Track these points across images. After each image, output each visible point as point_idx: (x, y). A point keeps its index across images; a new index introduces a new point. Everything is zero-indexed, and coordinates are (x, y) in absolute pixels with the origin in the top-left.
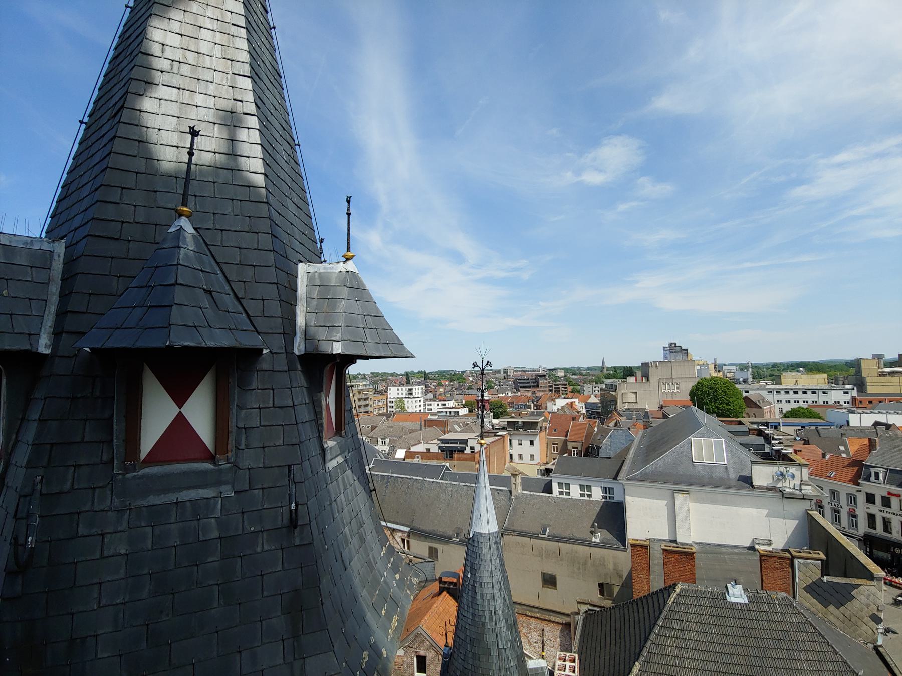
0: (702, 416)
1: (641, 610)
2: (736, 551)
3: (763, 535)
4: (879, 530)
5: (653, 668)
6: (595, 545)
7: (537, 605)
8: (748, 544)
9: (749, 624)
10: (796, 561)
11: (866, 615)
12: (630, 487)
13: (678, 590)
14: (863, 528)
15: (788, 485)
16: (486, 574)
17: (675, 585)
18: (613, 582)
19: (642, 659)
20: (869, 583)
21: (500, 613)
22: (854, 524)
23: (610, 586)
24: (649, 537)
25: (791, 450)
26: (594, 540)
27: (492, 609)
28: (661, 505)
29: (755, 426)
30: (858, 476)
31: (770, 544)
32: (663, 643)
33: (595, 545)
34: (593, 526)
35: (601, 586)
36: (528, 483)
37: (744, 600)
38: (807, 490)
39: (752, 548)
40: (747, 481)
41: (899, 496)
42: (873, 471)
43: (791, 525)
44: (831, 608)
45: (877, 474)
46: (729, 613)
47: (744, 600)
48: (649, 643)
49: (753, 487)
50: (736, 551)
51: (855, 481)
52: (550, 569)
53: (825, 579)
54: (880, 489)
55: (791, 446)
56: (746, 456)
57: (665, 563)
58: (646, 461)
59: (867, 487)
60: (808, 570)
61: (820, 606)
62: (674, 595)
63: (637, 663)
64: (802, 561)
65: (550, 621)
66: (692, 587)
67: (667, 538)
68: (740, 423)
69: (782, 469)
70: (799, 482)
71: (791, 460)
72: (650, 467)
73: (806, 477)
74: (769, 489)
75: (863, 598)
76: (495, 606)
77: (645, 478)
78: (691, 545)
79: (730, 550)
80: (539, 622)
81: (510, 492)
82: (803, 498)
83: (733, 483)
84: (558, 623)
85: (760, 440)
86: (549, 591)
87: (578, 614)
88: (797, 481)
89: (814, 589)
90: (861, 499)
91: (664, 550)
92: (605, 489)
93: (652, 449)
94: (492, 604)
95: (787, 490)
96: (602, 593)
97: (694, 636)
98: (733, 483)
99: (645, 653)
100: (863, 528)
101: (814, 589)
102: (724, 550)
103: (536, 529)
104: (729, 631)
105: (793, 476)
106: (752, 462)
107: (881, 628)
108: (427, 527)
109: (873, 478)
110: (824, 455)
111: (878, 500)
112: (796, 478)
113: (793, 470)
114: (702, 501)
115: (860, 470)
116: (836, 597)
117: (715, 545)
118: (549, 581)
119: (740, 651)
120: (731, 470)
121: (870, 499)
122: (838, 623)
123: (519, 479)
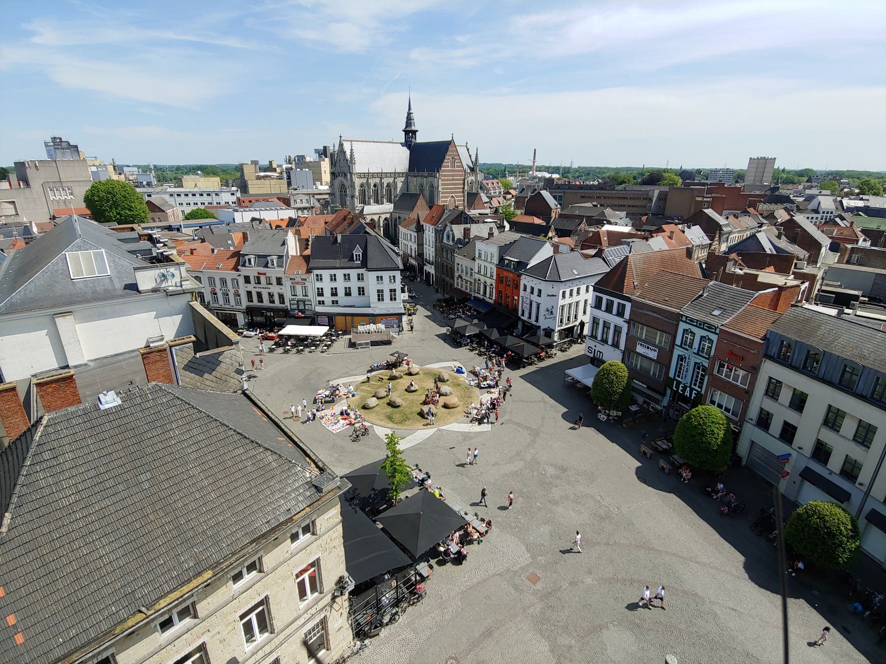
1: (10, 459)
2: (133, 354)
3: (155, 334)
4: (255, 302)
9: (126, 420)
10: (173, 349)
14: (245, 303)
15: (170, 285)
17: (41, 418)
19: (12, 506)
20: (230, 348)
22: (239, 303)
24: (34, 373)
25: (174, 252)
28: (41, 337)
29: (146, 232)
30: (237, 264)
31: (162, 339)
38: (188, 285)
39: (148, 346)
40: (133, 287)
42: (247, 258)
43: (178, 318)
44: (206, 375)
45: (250, 260)
49: (139, 292)
53: (198, 355)
54: (251, 271)
55: (175, 248)
56: (129, 262)
58: (14, 289)
59: (245, 271)
60: (184, 355)
61: (197, 377)
62: (41, 429)
64: (177, 348)
68: (132, 229)
69: (163, 271)
70: (179, 280)
74: (155, 291)
75: (227, 360)
78: (86, 365)
79: (127, 356)
82: (184, 292)
83: (121, 292)
88: (177, 279)
89: (193, 367)
90: (241, 280)
95: (170, 288)
98: (121, 292)
99: (15, 499)
100: (245, 303)
101: (193, 367)
102: (121, 358)
105: (173, 275)
106: (136, 269)
107: (244, 376)
109: (247, 264)
110: (213, 251)
112: (177, 277)
113: (172, 270)
114: (103, 316)
115: (239, 260)
117: (112, 356)
119: (118, 447)
120: (116, 281)
121: (247, 280)
122: (213, 385)
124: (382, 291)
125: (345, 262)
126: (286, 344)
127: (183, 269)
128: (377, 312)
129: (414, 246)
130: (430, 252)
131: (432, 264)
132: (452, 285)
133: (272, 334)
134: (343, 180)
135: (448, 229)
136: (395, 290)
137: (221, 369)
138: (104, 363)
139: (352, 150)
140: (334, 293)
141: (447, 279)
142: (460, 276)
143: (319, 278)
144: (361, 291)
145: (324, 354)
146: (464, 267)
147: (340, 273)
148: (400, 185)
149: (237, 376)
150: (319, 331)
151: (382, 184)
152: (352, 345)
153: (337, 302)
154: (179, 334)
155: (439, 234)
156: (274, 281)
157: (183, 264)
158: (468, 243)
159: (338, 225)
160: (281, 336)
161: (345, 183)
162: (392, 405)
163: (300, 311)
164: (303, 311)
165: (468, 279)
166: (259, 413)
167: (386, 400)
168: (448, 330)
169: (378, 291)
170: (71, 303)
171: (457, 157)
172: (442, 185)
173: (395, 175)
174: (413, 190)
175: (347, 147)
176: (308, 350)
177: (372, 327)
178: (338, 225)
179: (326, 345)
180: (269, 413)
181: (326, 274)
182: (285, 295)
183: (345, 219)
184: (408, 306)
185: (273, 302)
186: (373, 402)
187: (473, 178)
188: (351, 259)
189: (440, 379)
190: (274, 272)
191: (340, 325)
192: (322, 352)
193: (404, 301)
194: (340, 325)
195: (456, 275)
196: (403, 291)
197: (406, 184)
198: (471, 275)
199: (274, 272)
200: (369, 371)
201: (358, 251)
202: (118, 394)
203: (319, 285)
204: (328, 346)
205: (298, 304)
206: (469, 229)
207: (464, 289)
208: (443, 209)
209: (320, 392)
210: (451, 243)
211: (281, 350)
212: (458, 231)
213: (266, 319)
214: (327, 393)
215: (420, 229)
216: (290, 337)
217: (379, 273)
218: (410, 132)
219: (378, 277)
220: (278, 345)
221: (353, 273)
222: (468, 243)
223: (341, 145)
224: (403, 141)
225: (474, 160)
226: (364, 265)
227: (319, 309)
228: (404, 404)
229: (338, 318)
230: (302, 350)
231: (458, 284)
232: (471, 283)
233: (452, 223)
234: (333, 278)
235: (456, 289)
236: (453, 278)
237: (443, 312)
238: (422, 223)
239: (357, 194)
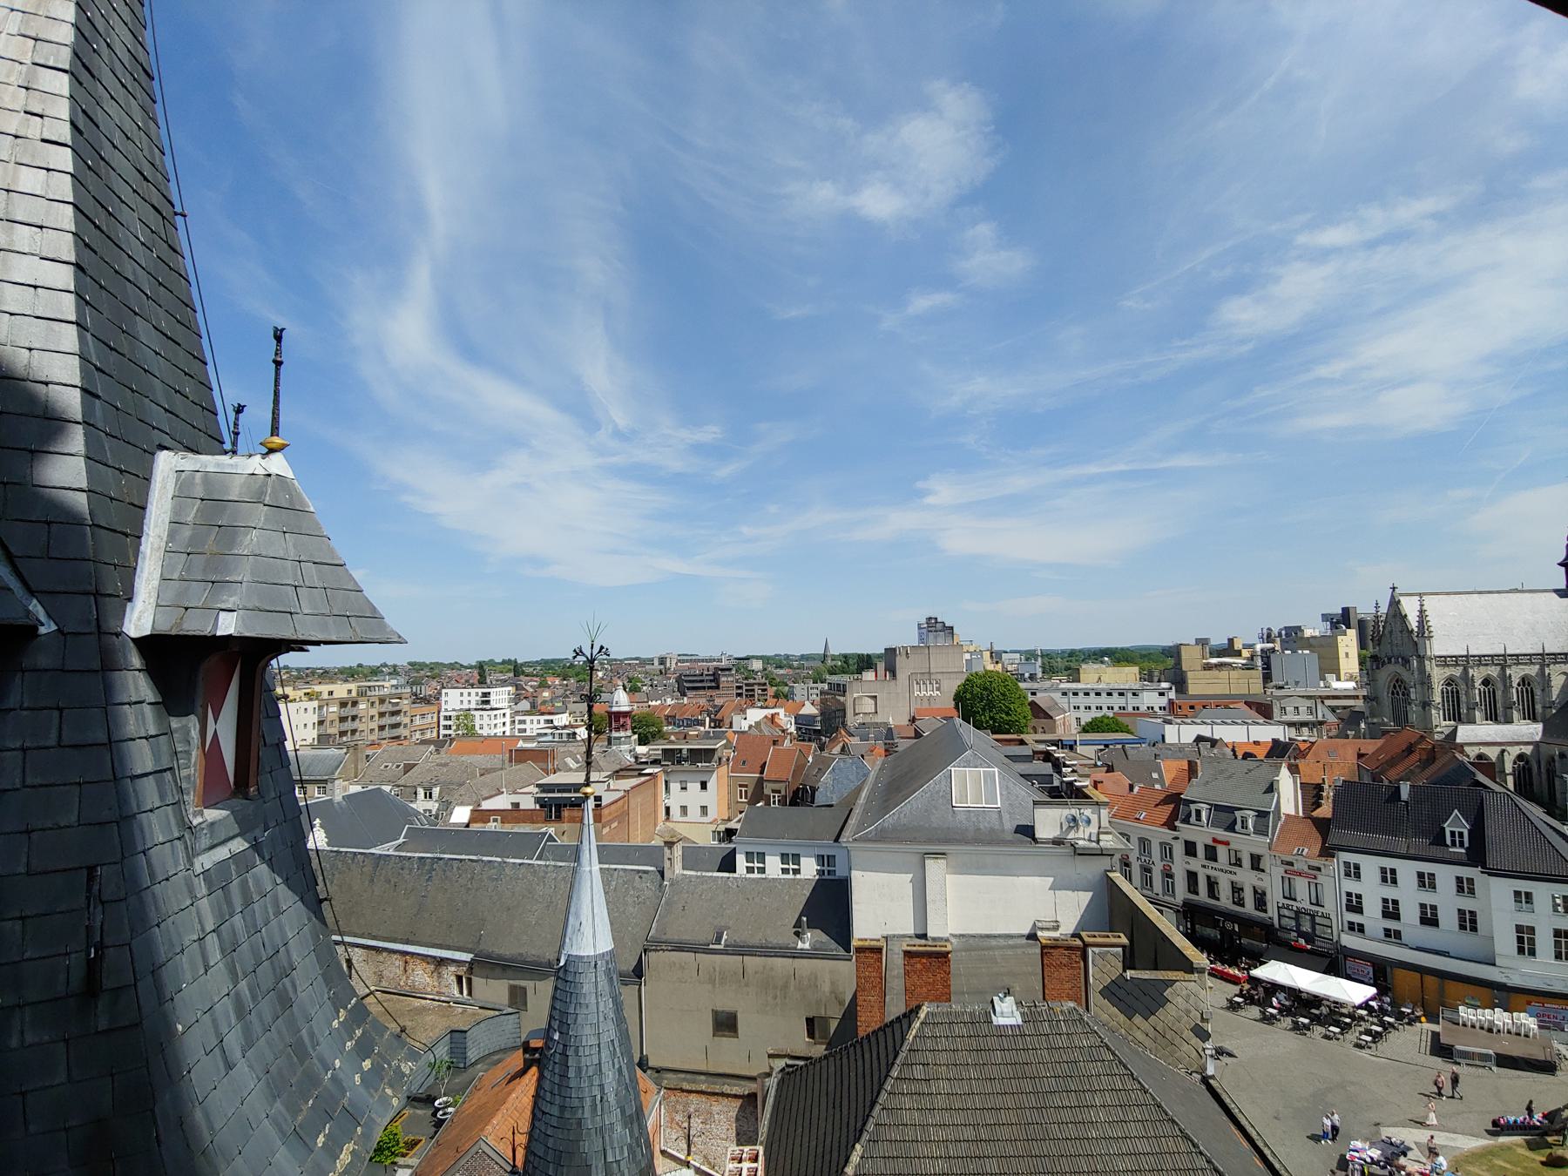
0: (968, 731)
1: (867, 1056)
2: (1011, 942)
3: (1046, 915)
4: (1203, 896)
5: (883, 1149)
6: (803, 955)
7: (703, 1068)
8: (1026, 931)
10: (1090, 950)
12: (859, 853)
13: (922, 1015)
14: (1181, 893)
16: (588, 1030)
17: (919, 1007)
18: (830, 1014)
19: (865, 1136)
20: (1187, 977)
21: (612, 1098)
22: (1169, 888)
23: (825, 1020)
26: (800, 945)
27: (596, 1092)
28: (902, 882)
29: (1042, 747)
31: (1056, 928)
32: (901, 1107)
33: (803, 955)
34: (798, 924)
35: (810, 1022)
36: (694, 857)
37: (1016, 1020)
38: (1108, 841)
39: (1032, 936)
40: (1027, 831)
41: (1227, 843)
42: (1193, 807)
43: (1085, 897)
44: (1138, 1019)
45: (1198, 813)
46: (993, 1042)
47: (1016, 1020)
48: (878, 1108)
49: (1035, 839)
50: (1011, 942)
51: (1170, 824)
52: (725, 1004)
53: (1129, 974)
54: (1202, 834)
55: (1088, 776)
56: (1026, 793)
57: (907, 973)
58: (885, 808)
59: (1187, 832)
60: (1105, 965)
61: (1122, 1018)
62: (916, 1025)
63: (858, 1146)
64: (1097, 950)
65: (723, 1095)
66: (944, 1007)
68: (1022, 742)
69: (1074, 811)
70: (1095, 831)
71: (1087, 797)
72: (889, 819)
73: (1105, 823)
74: (1057, 842)
75: (1180, 1000)
76: (601, 1086)
77: (882, 837)
79: (1002, 942)
80: (704, 1098)
81: (662, 873)
82: (1102, 853)
83: (1010, 836)
84: (735, 1096)
85: (1047, 768)
86: (726, 1042)
87: (769, 1075)
88: (1093, 829)
89: (1115, 992)
90: (1179, 849)
91: (907, 954)
92: (820, 859)
93: (896, 787)
94: (596, 1082)
95: (1081, 843)
96: (811, 1034)
97: (944, 1086)
99: (870, 1127)
100: (1181, 893)
101: (1115, 992)
102: (993, 942)
103: (703, 935)
104: (995, 1072)
105: (1089, 822)
108: (506, 948)
109: (1193, 819)
110: (1131, 788)
111: (1200, 851)
112: (1094, 826)
113: (1088, 812)
115: (1177, 808)
116: (1138, 1000)
117: (981, 936)
118: (726, 1024)
119: (1009, 1101)
120: (1006, 816)
121: (1190, 849)
122: (1148, 1042)
123: (678, 851)
125: (1421, 844)
126: (1264, 1003)
127: (1104, 812)
128: (1515, 980)
133: (1234, 971)
134: (1399, 669)
137: (1167, 1014)
138: (979, 943)
139: (1421, 611)
140: (1391, 910)
143: (1354, 872)
144: (1468, 921)
145: (1363, 1053)
147: (1407, 870)
149: (1195, 1041)
150: (1355, 993)
151: (1506, 680)
153: (1398, 934)
154: (1084, 924)
156: (1246, 862)
157: (1106, 804)
159: (1392, 762)
160: (1256, 982)
161: (1405, 675)
163: (1301, 934)
164: (1310, 938)
166: (1245, 1144)
170: (947, 841)
175: (1410, 608)
176: (1319, 1030)
177: (1500, 1017)
178: (1392, 762)
179: (1368, 1032)
180: (1267, 1151)
181: (1371, 866)
182: (1268, 897)
183: (1410, 750)
185: (1240, 902)
188: (1439, 839)
190: (1247, 843)
191: (1407, 991)
192: (1358, 1046)
194: (1407, 991)
199: (1247, 843)
201: (1456, 824)
202: (1019, 1004)
203: (1350, 886)
204: (1376, 1037)
205: (1297, 919)
209: (1358, 1144)
211: (1255, 1011)
213: (1234, 938)
214: (1375, 1153)
216: (1273, 988)
217: (1524, 886)
219: (1517, 894)
220: (1250, 1000)
221: (1446, 875)
223: (1395, 604)
226: (1477, 855)
227: (1350, 941)
230: (1306, 1027)
234: (1389, 877)
239: (1438, 699)
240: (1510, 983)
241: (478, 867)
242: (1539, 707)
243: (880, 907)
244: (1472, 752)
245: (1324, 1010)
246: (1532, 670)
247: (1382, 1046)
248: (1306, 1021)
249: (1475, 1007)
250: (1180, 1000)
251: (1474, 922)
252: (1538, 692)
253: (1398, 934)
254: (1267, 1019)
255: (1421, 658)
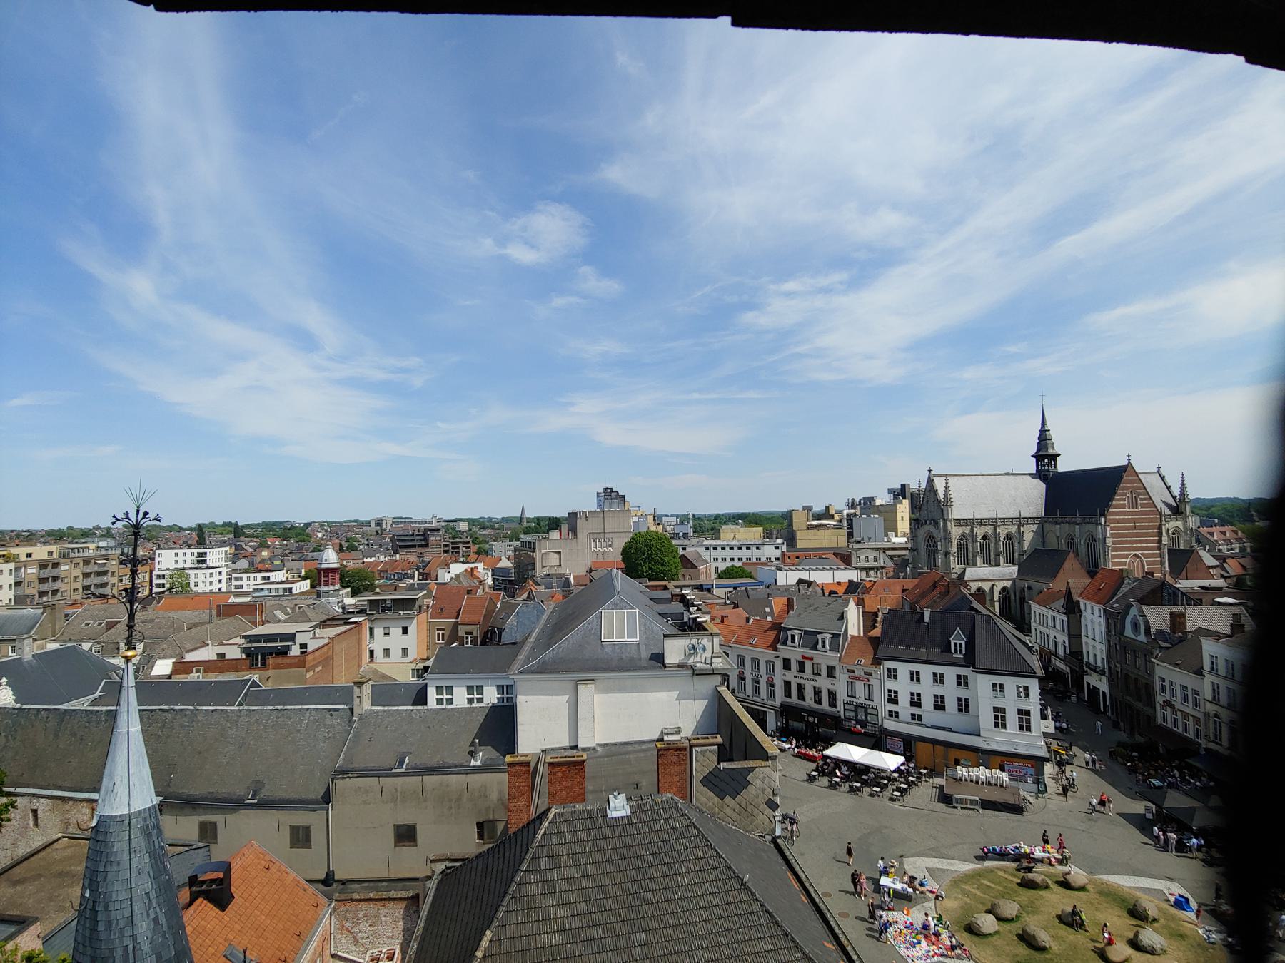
0: (621, 581)
2: (644, 747)
3: (671, 723)
4: (794, 699)
5: (511, 931)
6: (476, 770)
7: (385, 875)
8: (656, 737)
9: (630, 841)
11: (762, 799)
12: (522, 684)
13: (550, 816)
14: (780, 697)
15: (699, 660)
16: (118, 886)
18: (497, 817)
19: (496, 923)
20: (764, 763)
21: (146, 947)
22: (772, 695)
23: (493, 823)
24: (544, 747)
25: (708, 618)
26: (473, 763)
27: (128, 942)
28: (560, 702)
30: (776, 641)
32: (527, 892)
33: (476, 770)
34: (473, 744)
35: (480, 826)
36: (386, 693)
37: (626, 812)
38: (719, 663)
39: (661, 740)
40: (658, 658)
41: (811, 659)
42: (789, 633)
43: (701, 705)
44: (728, 799)
45: (793, 637)
46: (607, 832)
47: (626, 812)
48: (508, 897)
49: (664, 665)
50: (644, 747)
52: (405, 818)
53: (722, 765)
54: (794, 652)
57: (550, 781)
58: (549, 646)
59: (785, 652)
60: (705, 761)
61: (716, 799)
62: (546, 824)
63: (488, 932)
64: (699, 749)
65: (389, 899)
66: (579, 807)
67: (567, 744)
68: (665, 588)
69: (694, 641)
70: (709, 655)
71: (705, 630)
72: (549, 654)
73: (717, 649)
74: (681, 666)
75: (758, 781)
76: (134, 937)
77: (543, 669)
78: (594, 749)
79: (637, 747)
80: (372, 904)
81: (352, 710)
84: (401, 899)
85: (677, 607)
86: (407, 851)
87: (430, 878)
88: (708, 654)
90: (779, 664)
91: (550, 764)
92: (500, 688)
93: (558, 628)
94: (128, 933)
96: (481, 836)
97: (565, 872)
98: (644, 663)
99: (500, 914)
100: (780, 697)
102: (630, 748)
103: (387, 760)
104: (607, 856)
105: (704, 649)
106: (665, 636)
108: (198, 788)
109: (789, 642)
110: (748, 620)
111: (794, 665)
112: (708, 651)
113: (705, 641)
115: (779, 634)
116: (726, 785)
118: (406, 835)
120: (643, 648)
121: (787, 664)
122: (735, 816)
123: (367, 689)
124: (1003, 710)
125: (936, 652)
127: (716, 640)
128: (993, 747)
129: (1062, 638)
130: (1095, 648)
131: (1102, 672)
132: (1151, 719)
133: (813, 752)
134: (931, 528)
135: (1134, 612)
136: (1028, 713)
137: (749, 793)
138: (616, 751)
140: (916, 701)
141: (1139, 705)
142: (1168, 704)
143: (893, 674)
144: (964, 705)
145: (895, 805)
146: (1178, 688)
147: (926, 671)
148: (1028, 537)
149: (768, 811)
150: (891, 761)
151: (997, 535)
152: (946, 799)
153: (920, 717)
155: (1114, 621)
156: (824, 672)
157: (717, 635)
158: (1181, 640)
159: (923, 595)
161: (935, 533)
162: (1026, 939)
163: (858, 722)
164: (863, 724)
165: (1190, 711)
166: (796, 886)
167: (1016, 928)
168: (1148, 809)
169: (996, 709)
170: (596, 670)
171: (1140, 489)
172: (1113, 536)
173: (1021, 521)
174: (1053, 544)
175: (939, 485)
176: (867, 790)
177: (983, 773)
178: (923, 595)
179: (898, 789)
180: (811, 890)
181: (904, 669)
183: (935, 586)
184: (1054, 745)
185: (819, 702)
186: (987, 923)
187: (1180, 524)
189: (1136, 913)
190: (825, 657)
192: (892, 800)
193: (1046, 735)
195: (1160, 699)
196: (1044, 717)
197: (1041, 535)
198: (1196, 704)
199: (825, 657)
200: (980, 859)
201: (958, 639)
202: (629, 799)
203: (890, 685)
204: (904, 792)
205: (856, 711)
206: (1183, 615)
207: (1180, 730)
208: (1120, 576)
210: (1142, 638)
211: (825, 781)
212: (1158, 617)
213: (809, 728)
215: (1072, 609)
216: (839, 763)
217: (998, 679)
218: (1044, 456)
219: (994, 685)
220: (822, 773)
221: (950, 673)
222: (1181, 640)
223: (930, 481)
224: (1034, 471)
225: (1177, 492)
226: (970, 660)
227: (890, 725)
228: (1055, 947)
229: (921, 745)
230: (858, 789)
231: (1163, 717)
232: (1197, 720)
233: (1143, 601)
234: (915, 677)
235: (1161, 727)
236: (1151, 703)
237: (1132, 770)
238: (1076, 598)
239: (955, 550)
240: (989, 748)
241: (169, 716)
242: (1016, 555)
243: (542, 725)
244: (974, 587)
245: (872, 775)
246: (1013, 529)
247: (907, 798)
248: (858, 785)
249: (967, 766)
250: (758, 781)
251: (967, 706)
252: (1016, 544)
253: (920, 717)
254: (833, 786)
255: (945, 521)
